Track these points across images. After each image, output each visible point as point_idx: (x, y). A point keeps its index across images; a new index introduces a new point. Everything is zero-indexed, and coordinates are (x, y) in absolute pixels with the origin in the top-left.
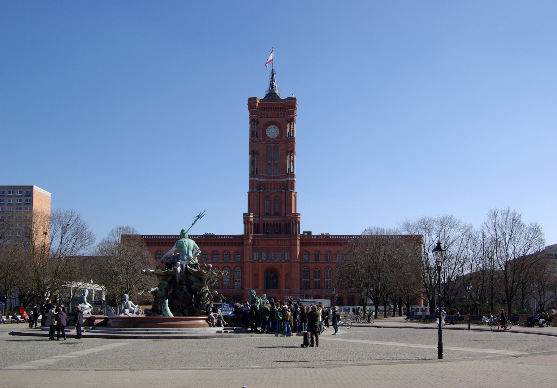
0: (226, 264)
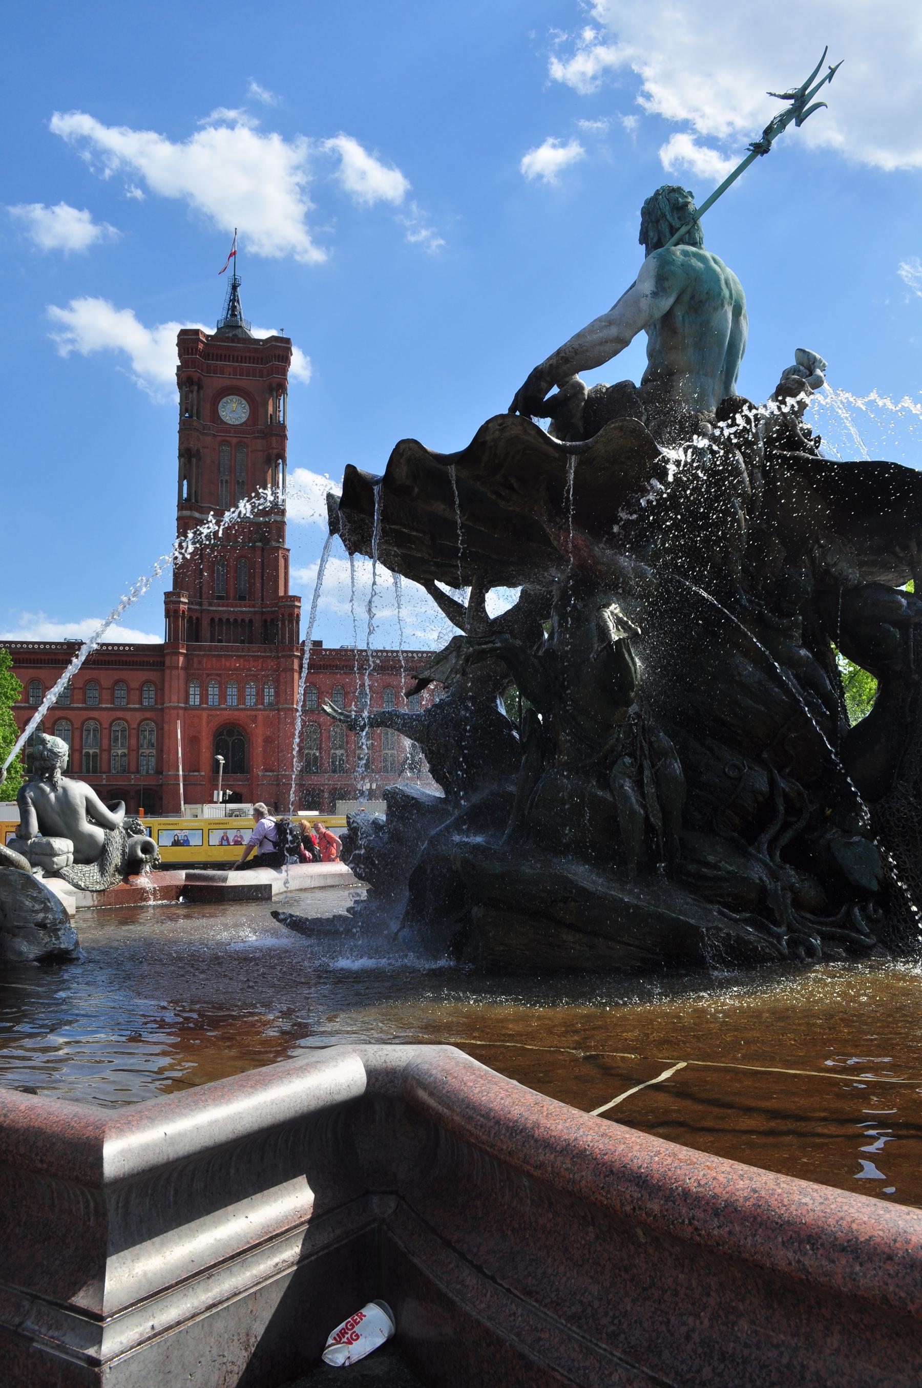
0: (119, 714)
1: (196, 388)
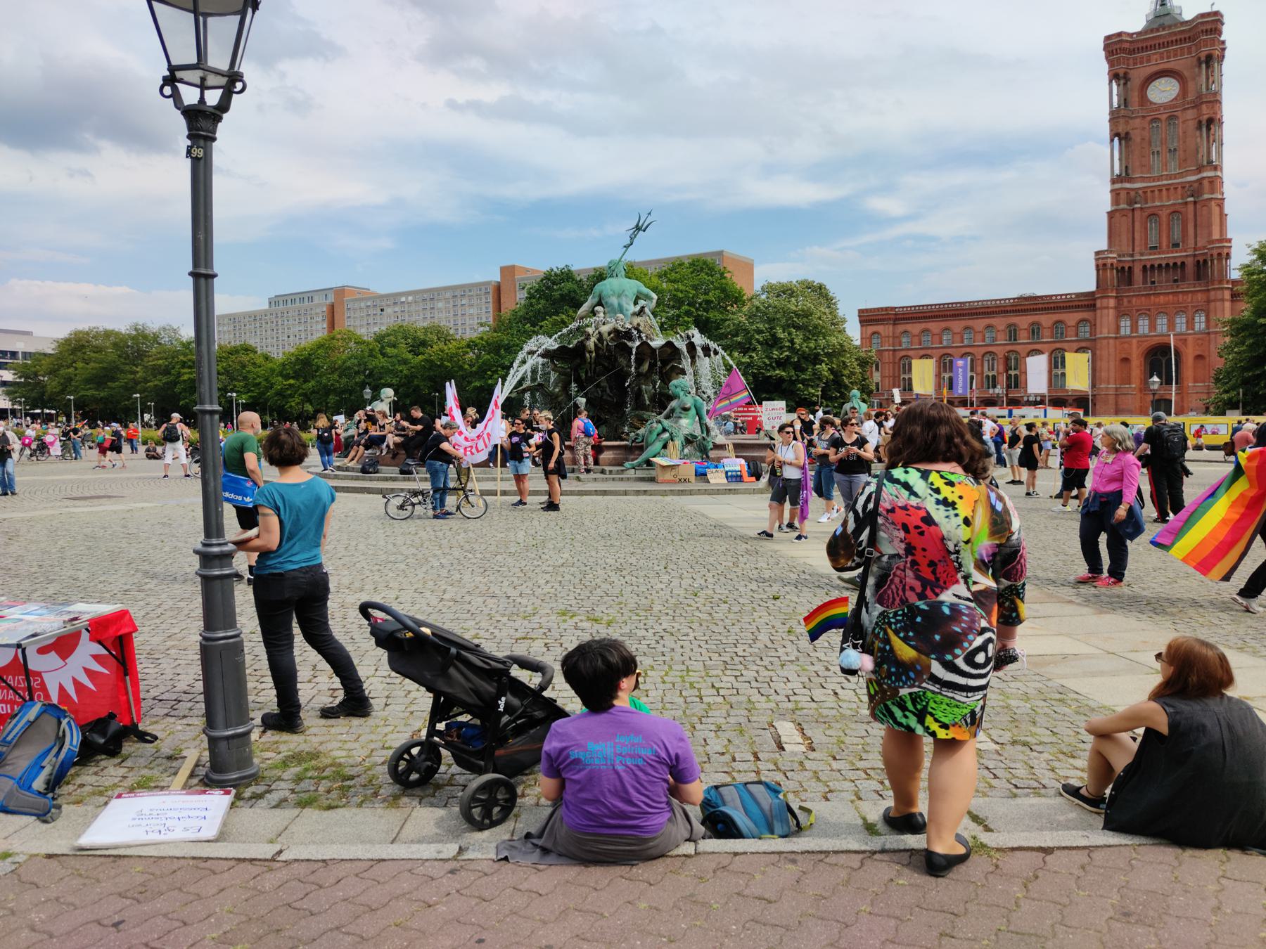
1: (1122, 82)
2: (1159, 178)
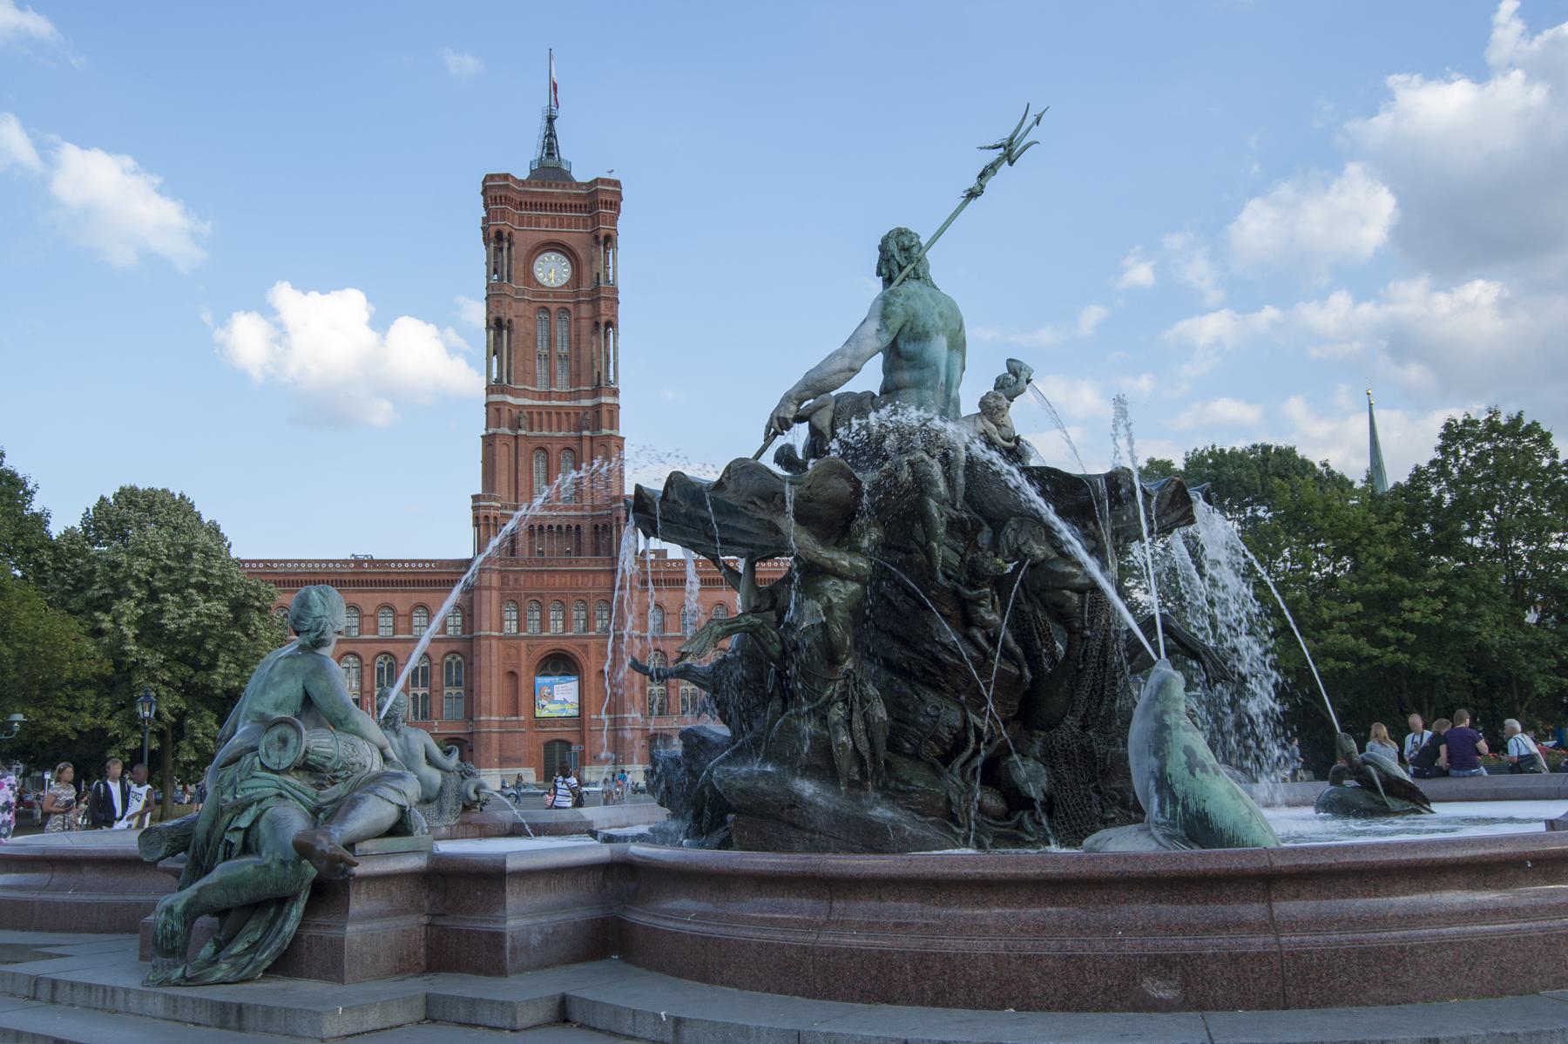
1: (506, 245)
2: (548, 395)
